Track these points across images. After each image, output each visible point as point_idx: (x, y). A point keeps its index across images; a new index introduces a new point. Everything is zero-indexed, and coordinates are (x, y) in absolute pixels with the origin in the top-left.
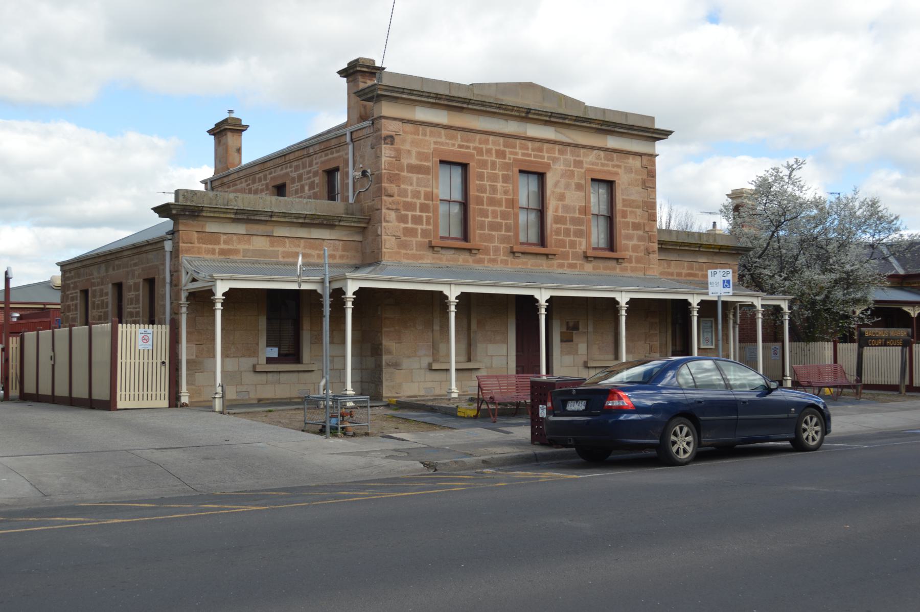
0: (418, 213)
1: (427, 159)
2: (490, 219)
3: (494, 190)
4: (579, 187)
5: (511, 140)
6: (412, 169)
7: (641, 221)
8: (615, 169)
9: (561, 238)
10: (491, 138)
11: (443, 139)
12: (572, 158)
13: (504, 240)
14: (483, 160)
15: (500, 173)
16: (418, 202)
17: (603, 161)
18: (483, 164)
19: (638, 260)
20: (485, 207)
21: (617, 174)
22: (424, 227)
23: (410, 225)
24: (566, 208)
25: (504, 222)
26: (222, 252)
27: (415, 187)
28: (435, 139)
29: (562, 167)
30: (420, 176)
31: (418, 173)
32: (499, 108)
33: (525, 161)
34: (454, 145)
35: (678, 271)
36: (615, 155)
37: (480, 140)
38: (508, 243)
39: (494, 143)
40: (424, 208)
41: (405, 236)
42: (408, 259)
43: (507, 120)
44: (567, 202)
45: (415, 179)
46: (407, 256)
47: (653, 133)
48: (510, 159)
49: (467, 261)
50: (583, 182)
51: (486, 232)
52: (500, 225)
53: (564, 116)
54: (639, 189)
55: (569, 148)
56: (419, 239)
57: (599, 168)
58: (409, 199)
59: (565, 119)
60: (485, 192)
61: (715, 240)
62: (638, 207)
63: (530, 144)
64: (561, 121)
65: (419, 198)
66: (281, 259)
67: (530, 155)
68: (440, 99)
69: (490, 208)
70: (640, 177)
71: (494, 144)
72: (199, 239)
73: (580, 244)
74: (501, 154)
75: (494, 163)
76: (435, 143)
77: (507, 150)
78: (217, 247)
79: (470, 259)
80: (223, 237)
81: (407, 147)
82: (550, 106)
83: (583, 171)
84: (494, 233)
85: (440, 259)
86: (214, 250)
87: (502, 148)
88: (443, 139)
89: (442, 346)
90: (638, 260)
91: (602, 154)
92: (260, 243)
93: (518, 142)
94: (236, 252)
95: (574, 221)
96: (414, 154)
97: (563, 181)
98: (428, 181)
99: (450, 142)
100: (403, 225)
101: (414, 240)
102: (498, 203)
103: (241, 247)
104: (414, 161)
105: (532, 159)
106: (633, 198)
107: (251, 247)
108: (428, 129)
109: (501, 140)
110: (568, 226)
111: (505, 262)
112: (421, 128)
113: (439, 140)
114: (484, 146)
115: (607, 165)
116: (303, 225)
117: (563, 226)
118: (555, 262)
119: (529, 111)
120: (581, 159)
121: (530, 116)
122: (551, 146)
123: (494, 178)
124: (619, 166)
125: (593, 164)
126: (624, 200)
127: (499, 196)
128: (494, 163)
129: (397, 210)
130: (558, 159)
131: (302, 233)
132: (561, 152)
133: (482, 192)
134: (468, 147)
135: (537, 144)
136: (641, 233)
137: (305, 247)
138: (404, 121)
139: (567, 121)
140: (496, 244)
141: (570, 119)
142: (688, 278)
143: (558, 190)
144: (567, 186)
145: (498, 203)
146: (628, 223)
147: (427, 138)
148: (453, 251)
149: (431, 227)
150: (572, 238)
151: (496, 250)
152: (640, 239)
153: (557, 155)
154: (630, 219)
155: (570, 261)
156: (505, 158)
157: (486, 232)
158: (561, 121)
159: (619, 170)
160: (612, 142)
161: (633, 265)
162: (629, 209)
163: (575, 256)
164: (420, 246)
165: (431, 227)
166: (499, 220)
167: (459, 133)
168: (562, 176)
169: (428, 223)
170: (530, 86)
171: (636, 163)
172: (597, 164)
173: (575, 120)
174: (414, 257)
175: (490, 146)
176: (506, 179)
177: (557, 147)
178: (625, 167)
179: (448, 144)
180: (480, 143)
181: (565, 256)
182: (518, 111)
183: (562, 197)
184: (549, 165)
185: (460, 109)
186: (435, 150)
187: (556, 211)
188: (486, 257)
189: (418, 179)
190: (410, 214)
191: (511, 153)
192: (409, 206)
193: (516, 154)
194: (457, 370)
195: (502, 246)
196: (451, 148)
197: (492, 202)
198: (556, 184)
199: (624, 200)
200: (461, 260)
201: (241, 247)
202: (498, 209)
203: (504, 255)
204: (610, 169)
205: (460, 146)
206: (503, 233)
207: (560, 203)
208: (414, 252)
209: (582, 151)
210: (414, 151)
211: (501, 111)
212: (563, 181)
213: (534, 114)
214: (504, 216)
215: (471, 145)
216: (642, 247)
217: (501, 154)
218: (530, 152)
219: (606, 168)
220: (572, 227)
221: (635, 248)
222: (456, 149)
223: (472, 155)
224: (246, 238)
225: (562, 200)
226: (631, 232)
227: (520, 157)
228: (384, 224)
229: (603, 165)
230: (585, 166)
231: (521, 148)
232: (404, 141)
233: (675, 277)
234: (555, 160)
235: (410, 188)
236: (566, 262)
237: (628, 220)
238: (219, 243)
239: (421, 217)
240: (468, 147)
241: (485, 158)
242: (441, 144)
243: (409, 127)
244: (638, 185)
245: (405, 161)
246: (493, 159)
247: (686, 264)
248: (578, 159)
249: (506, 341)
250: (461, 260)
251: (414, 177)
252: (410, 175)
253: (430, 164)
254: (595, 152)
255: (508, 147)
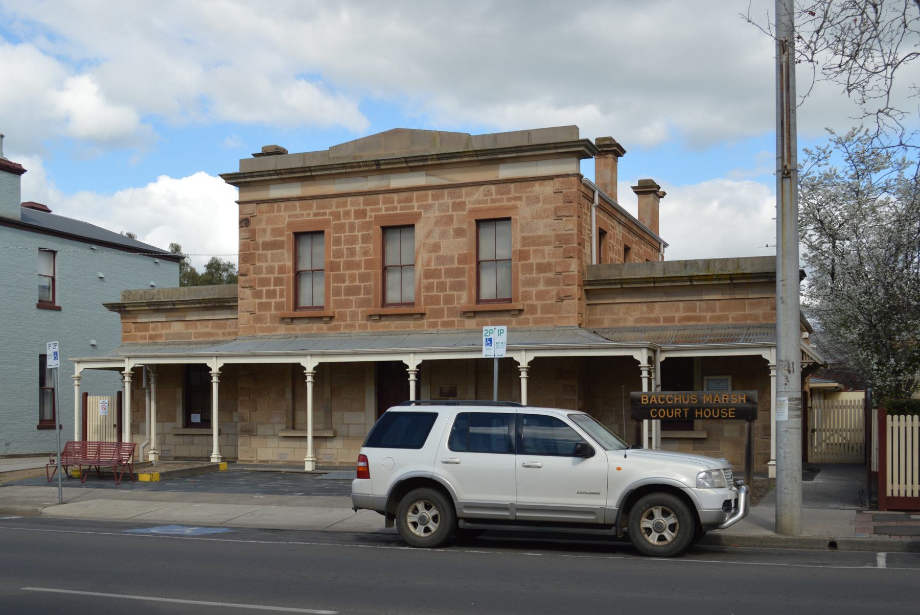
0: (272, 287)
1: (281, 234)
2: (347, 284)
3: (352, 252)
4: (459, 233)
5: (387, 195)
6: (267, 246)
7: (553, 260)
8: (513, 203)
9: (435, 293)
10: (349, 199)
11: (298, 211)
12: (450, 202)
13: (361, 304)
14: (340, 224)
15: (360, 234)
16: (272, 276)
17: (494, 196)
18: (340, 228)
19: (546, 309)
20: (342, 272)
21: (514, 208)
22: (278, 300)
23: (264, 300)
24: (441, 260)
25: (362, 285)
26: (152, 337)
27: (269, 263)
28: (290, 213)
29: (437, 214)
30: (274, 251)
31: (272, 249)
32: (344, 168)
33: (390, 216)
34: (309, 215)
35: (669, 314)
36: (512, 186)
37: (337, 203)
38: (367, 307)
39: (353, 204)
40: (278, 281)
41: (260, 310)
42: (263, 332)
43: (366, 177)
44: (442, 252)
45: (269, 256)
46: (262, 330)
47: (555, 148)
48: (371, 217)
49: (322, 329)
50: (465, 226)
51: (343, 297)
52: (359, 288)
53: (424, 158)
54: (551, 221)
55: (446, 191)
56: (273, 312)
57: (489, 205)
58: (264, 276)
59: (426, 160)
60: (342, 256)
61: (738, 267)
62: (547, 243)
63: (395, 196)
64: (421, 163)
65: (273, 273)
66: (193, 340)
67: (396, 208)
68: (281, 174)
69: (347, 273)
70: (551, 206)
71: (351, 205)
72: (135, 328)
73: (459, 298)
74: (361, 214)
75: (352, 226)
76: (289, 216)
77: (368, 208)
78: (147, 334)
79: (325, 327)
80: (151, 325)
81: (263, 226)
82: (419, 150)
83: (465, 213)
84: (351, 298)
85: (294, 330)
86: (673, 318)
87: (362, 207)
88: (298, 211)
89: (299, 414)
90: (546, 309)
91: (493, 188)
92: (178, 327)
93: (381, 197)
94: (160, 336)
95: (450, 273)
96: (269, 231)
97: (437, 230)
98: (283, 255)
99: (305, 212)
100: (258, 301)
101: (268, 313)
102: (357, 265)
103: (164, 332)
104: (268, 238)
105: (399, 212)
106: (539, 233)
107: (171, 332)
108: (283, 205)
109: (361, 199)
110: (443, 279)
111: (364, 327)
112: (276, 205)
113: (294, 213)
114: (341, 210)
115: (501, 200)
116: (207, 309)
117: (436, 281)
118: (425, 321)
119: (377, 163)
120: (463, 199)
121: (383, 167)
122: (423, 192)
123: (352, 240)
124: (520, 199)
125: (479, 203)
126: (524, 238)
127: (357, 258)
128: (352, 226)
129: (251, 287)
130: (431, 206)
131: (208, 316)
132: (435, 198)
133: (339, 257)
134: (324, 214)
135: (404, 195)
136: (551, 275)
137: (212, 328)
138: (259, 202)
139: (429, 163)
140: (354, 309)
141: (432, 159)
142: (685, 323)
143: (431, 241)
144: (443, 235)
145: (357, 265)
146: (531, 265)
147: (282, 213)
148: (307, 321)
149: (284, 299)
150: (448, 292)
151: (354, 315)
152: (549, 282)
153: (430, 201)
154: (534, 260)
155: (446, 319)
156: (365, 217)
157: (343, 297)
158: (421, 163)
159: (518, 203)
160: (506, 172)
161: (539, 315)
162: (532, 248)
163: (452, 312)
164: (273, 318)
165: (284, 299)
166: (357, 283)
167: (315, 201)
168: (436, 224)
169: (281, 296)
170: (396, 133)
171: (548, 189)
172: (484, 202)
173: (439, 159)
174: (268, 329)
175: (349, 208)
176: (366, 239)
177: (430, 192)
178: (528, 198)
179: (302, 215)
180: (337, 207)
181: (439, 313)
182: (366, 166)
183: (436, 248)
184: (419, 214)
185: (312, 178)
186: (289, 224)
187: (428, 264)
188: (342, 323)
189: (272, 254)
190: (264, 289)
191: (372, 210)
192: (264, 282)
193: (379, 210)
194: (314, 438)
195: (360, 310)
196: (305, 218)
197: (350, 265)
198: (429, 235)
199: (524, 238)
200: (315, 328)
201: (164, 332)
202: (356, 272)
203: (362, 320)
204: (505, 203)
205: (316, 215)
206: (362, 296)
207: (433, 255)
208: (268, 325)
209: (464, 190)
210: (269, 229)
211: (348, 170)
212: (437, 230)
213: (387, 164)
214: (364, 278)
215: (328, 211)
216: (554, 293)
217: (361, 214)
218: (396, 204)
219: (497, 204)
220: (448, 280)
221: (541, 295)
222: (311, 218)
223: (327, 222)
224: (167, 324)
225: (434, 251)
226: (535, 275)
227: (383, 212)
228: (239, 302)
229: (493, 201)
230: (468, 206)
231: (384, 203)
232: (260, 221)
233: (662, 323)
234: (427, 208)
235: (264, 265)
236: (439, 320)
237: (531, 261)
238: (148, 330)
239: (275, 291)
240: (324, 214)
241: (342, 221)
242: (297, 216)
243: (263, 207)
244: (547, 217)
245: (260, 240)
246: (352, 220)
247: (681, 304)
248: (458, 200)
249: (362, 409)
250: (315, 328)
251: (269, 253)
252: (265, 252)
253: (284, 238)
254: (482, 188)
255: (368, 205)
